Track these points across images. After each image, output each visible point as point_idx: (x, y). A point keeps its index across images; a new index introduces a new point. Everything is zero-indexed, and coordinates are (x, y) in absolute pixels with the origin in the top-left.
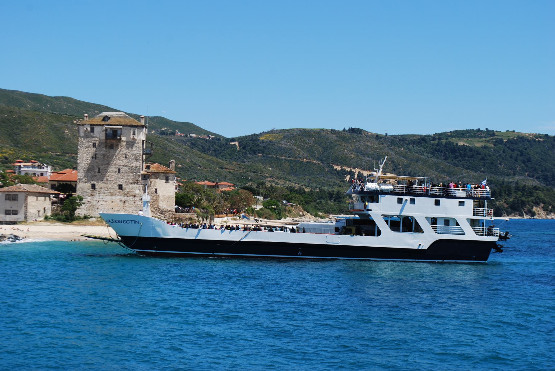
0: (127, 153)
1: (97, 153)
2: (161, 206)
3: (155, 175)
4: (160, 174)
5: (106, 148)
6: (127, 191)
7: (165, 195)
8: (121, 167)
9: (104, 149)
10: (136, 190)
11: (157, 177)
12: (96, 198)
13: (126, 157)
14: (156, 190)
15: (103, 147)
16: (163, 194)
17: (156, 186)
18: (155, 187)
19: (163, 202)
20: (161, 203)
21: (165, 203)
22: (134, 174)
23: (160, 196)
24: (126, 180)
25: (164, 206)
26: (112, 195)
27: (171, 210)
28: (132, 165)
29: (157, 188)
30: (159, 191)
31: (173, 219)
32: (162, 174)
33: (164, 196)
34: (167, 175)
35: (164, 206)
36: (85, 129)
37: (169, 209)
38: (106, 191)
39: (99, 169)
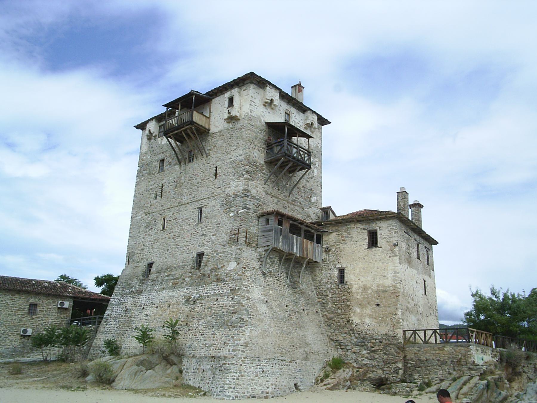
0: (218, 164)
1: (164, 181)
2: (356, 320)
3: (338, 231)
4: (352, 225)
5: (180, 166)
6: (210, 268)
7: (368, 285)
8: (204, 203)
9: (177, 167)
10: (229, 262)
11: (344, 234)
12: (143, 299)
13: (216, 174)
14: (342, 272)
15: (175, 165)
16: (361, 285)
17: (341, 260)
18: (338, 266)
19: (362, 306)
20: (358, 310)
21: (368, 311)
22: (232, 214)
23: (354, 289)
24: (213, 238)
25: (368, 321)
26: (175, 285)
27: (391, 333)
28: (227, 190)
29: (344, 266)
30: (352, 276)
31: (400, 365)
32: (359, 225)
33: (365, 288)
34: (374, 226)
35: (368, 321)
36: (147, 132)
37: (384, 330)
38: (167, 278)
39: (164, 219)
